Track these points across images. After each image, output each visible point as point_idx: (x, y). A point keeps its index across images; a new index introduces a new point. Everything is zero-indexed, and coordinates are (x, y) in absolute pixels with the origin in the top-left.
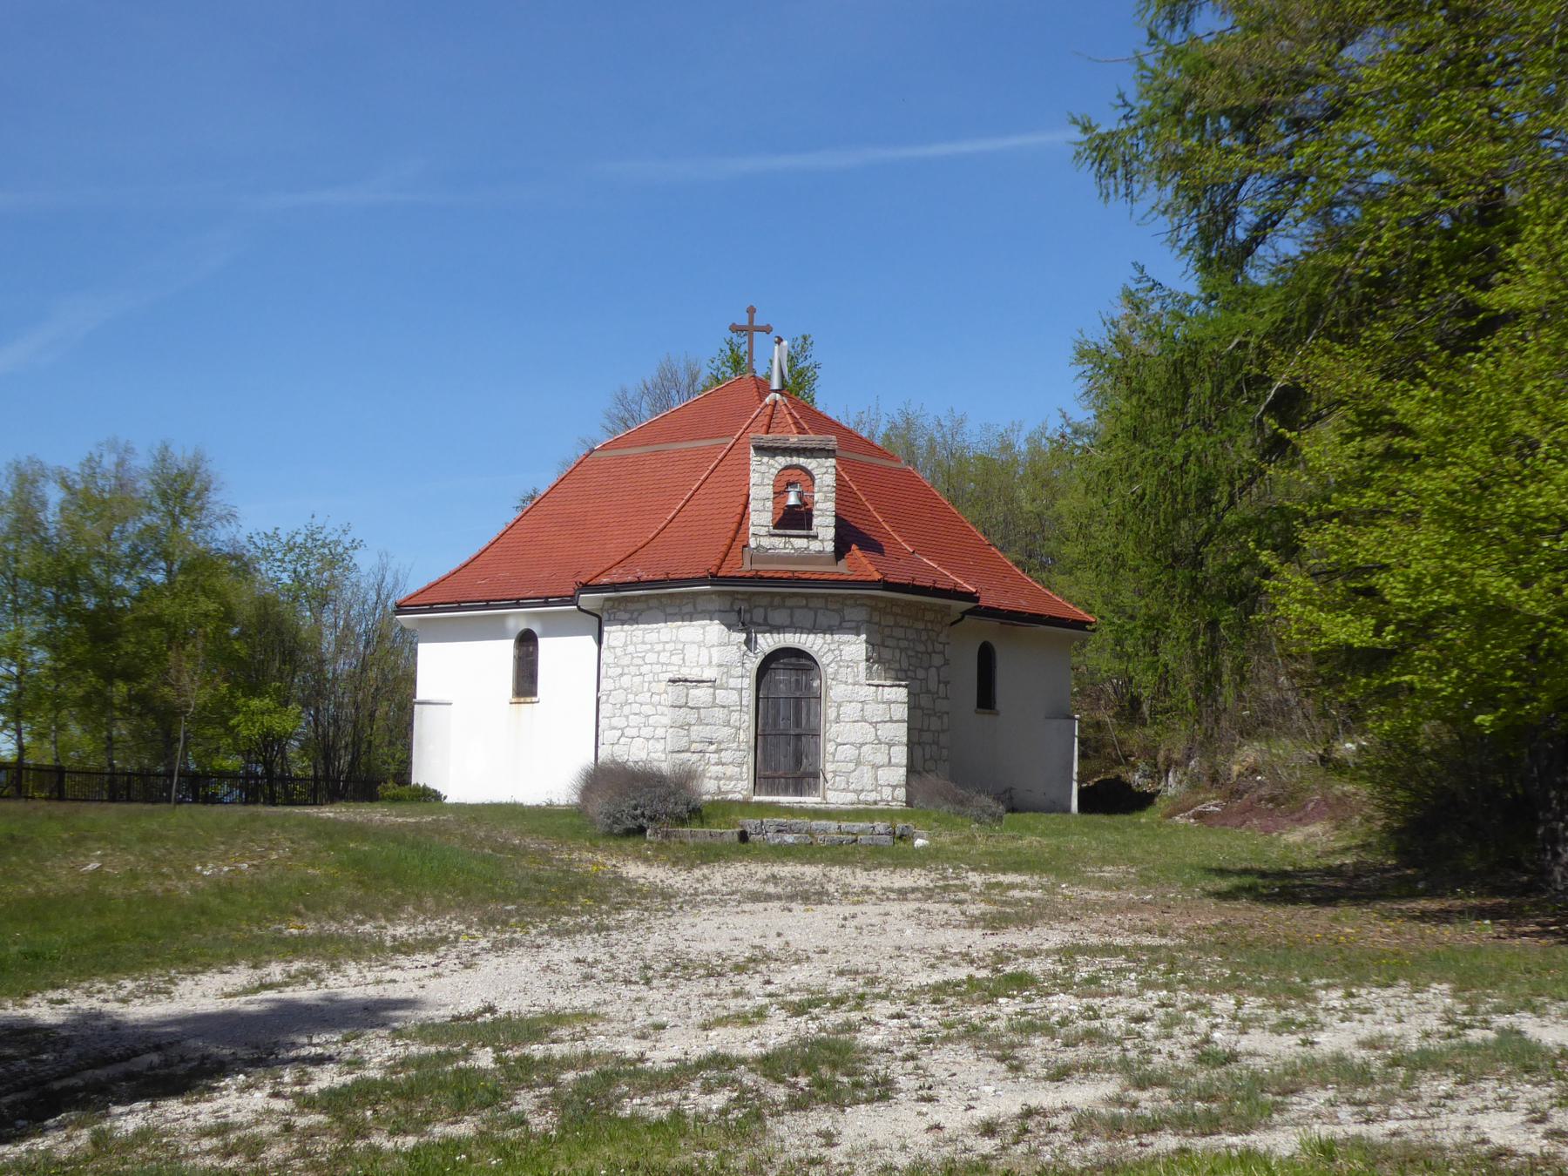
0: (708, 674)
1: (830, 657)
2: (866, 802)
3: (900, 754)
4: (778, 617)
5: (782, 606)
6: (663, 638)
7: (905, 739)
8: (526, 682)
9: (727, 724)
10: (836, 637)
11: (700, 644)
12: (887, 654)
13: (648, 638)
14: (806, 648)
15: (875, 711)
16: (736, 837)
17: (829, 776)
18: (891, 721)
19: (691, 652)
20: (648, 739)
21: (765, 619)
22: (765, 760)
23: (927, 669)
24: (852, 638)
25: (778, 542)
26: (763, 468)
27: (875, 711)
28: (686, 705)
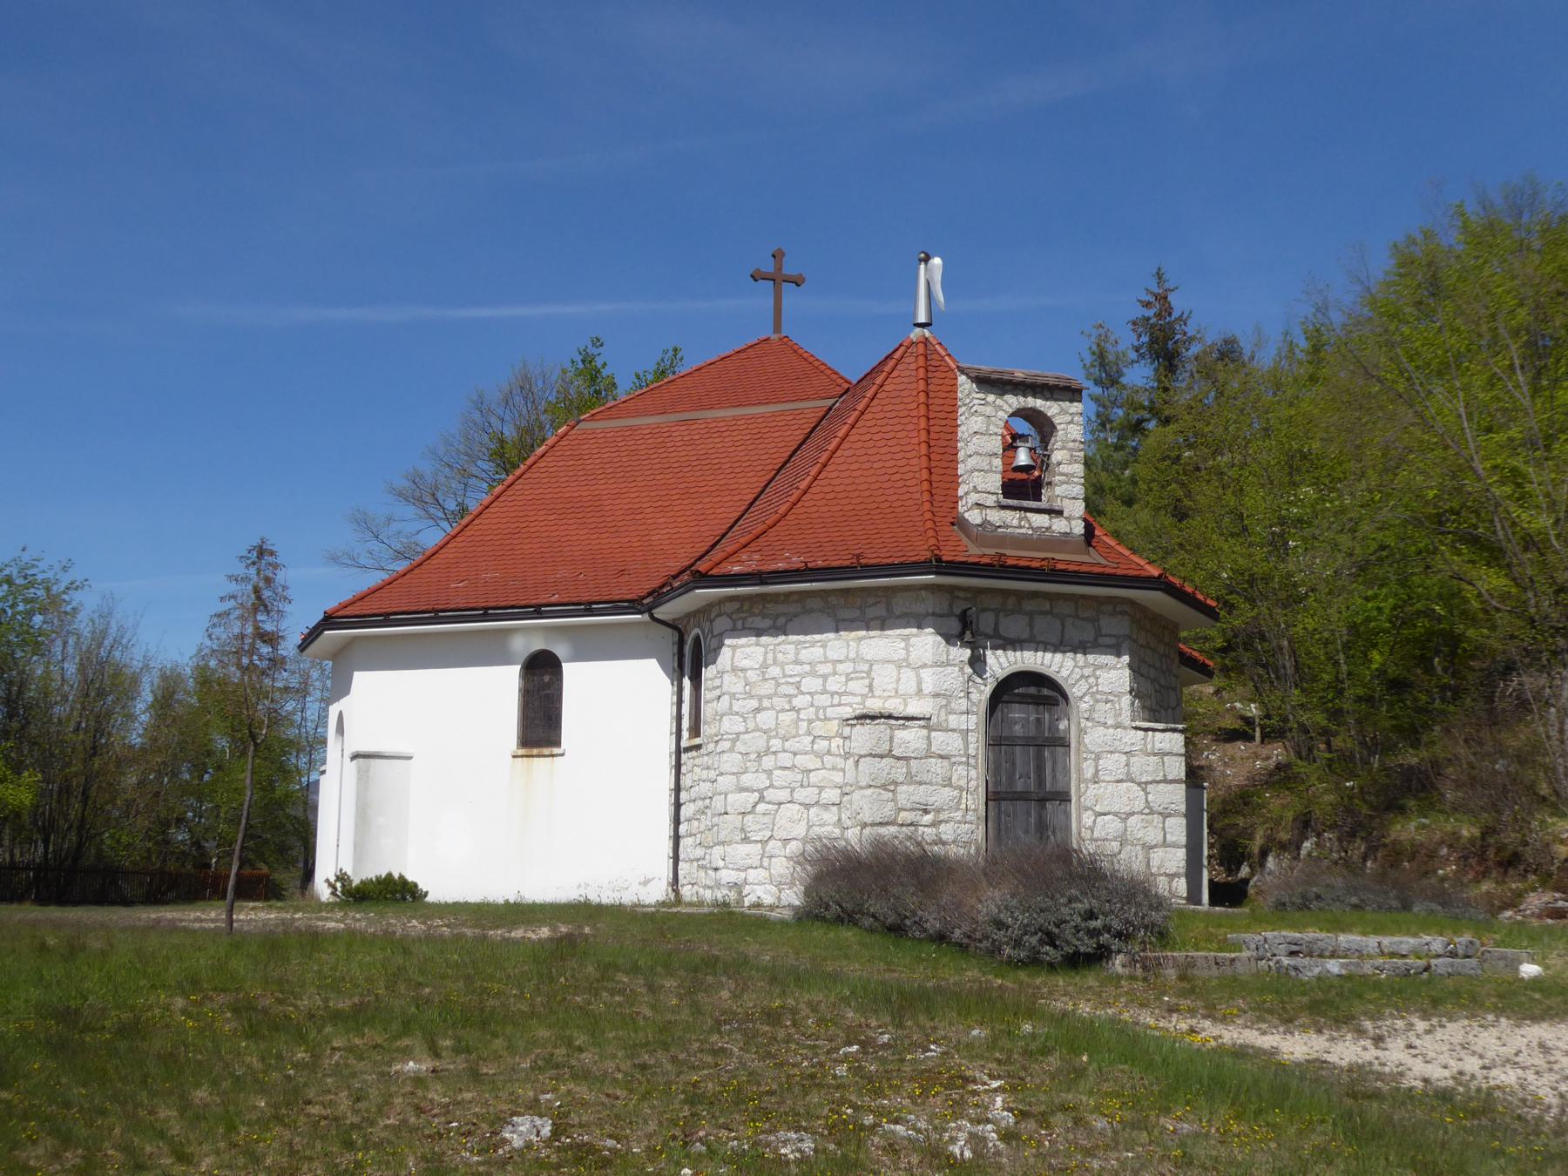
0: (913, 709)
4: (1014, 626)
6: (832, 655)
8: (540, 724)
9: (948, 783)
10: (1091, 658)
13: (805, 654)
14: (1050, 673)
15: (1145, 767)
18: (1165, 781)
19: (885, 677)
21: (996, 628)
25: (1012, 518)
26: (988, 410)
27: (1145, 767)
28: (889, 754)
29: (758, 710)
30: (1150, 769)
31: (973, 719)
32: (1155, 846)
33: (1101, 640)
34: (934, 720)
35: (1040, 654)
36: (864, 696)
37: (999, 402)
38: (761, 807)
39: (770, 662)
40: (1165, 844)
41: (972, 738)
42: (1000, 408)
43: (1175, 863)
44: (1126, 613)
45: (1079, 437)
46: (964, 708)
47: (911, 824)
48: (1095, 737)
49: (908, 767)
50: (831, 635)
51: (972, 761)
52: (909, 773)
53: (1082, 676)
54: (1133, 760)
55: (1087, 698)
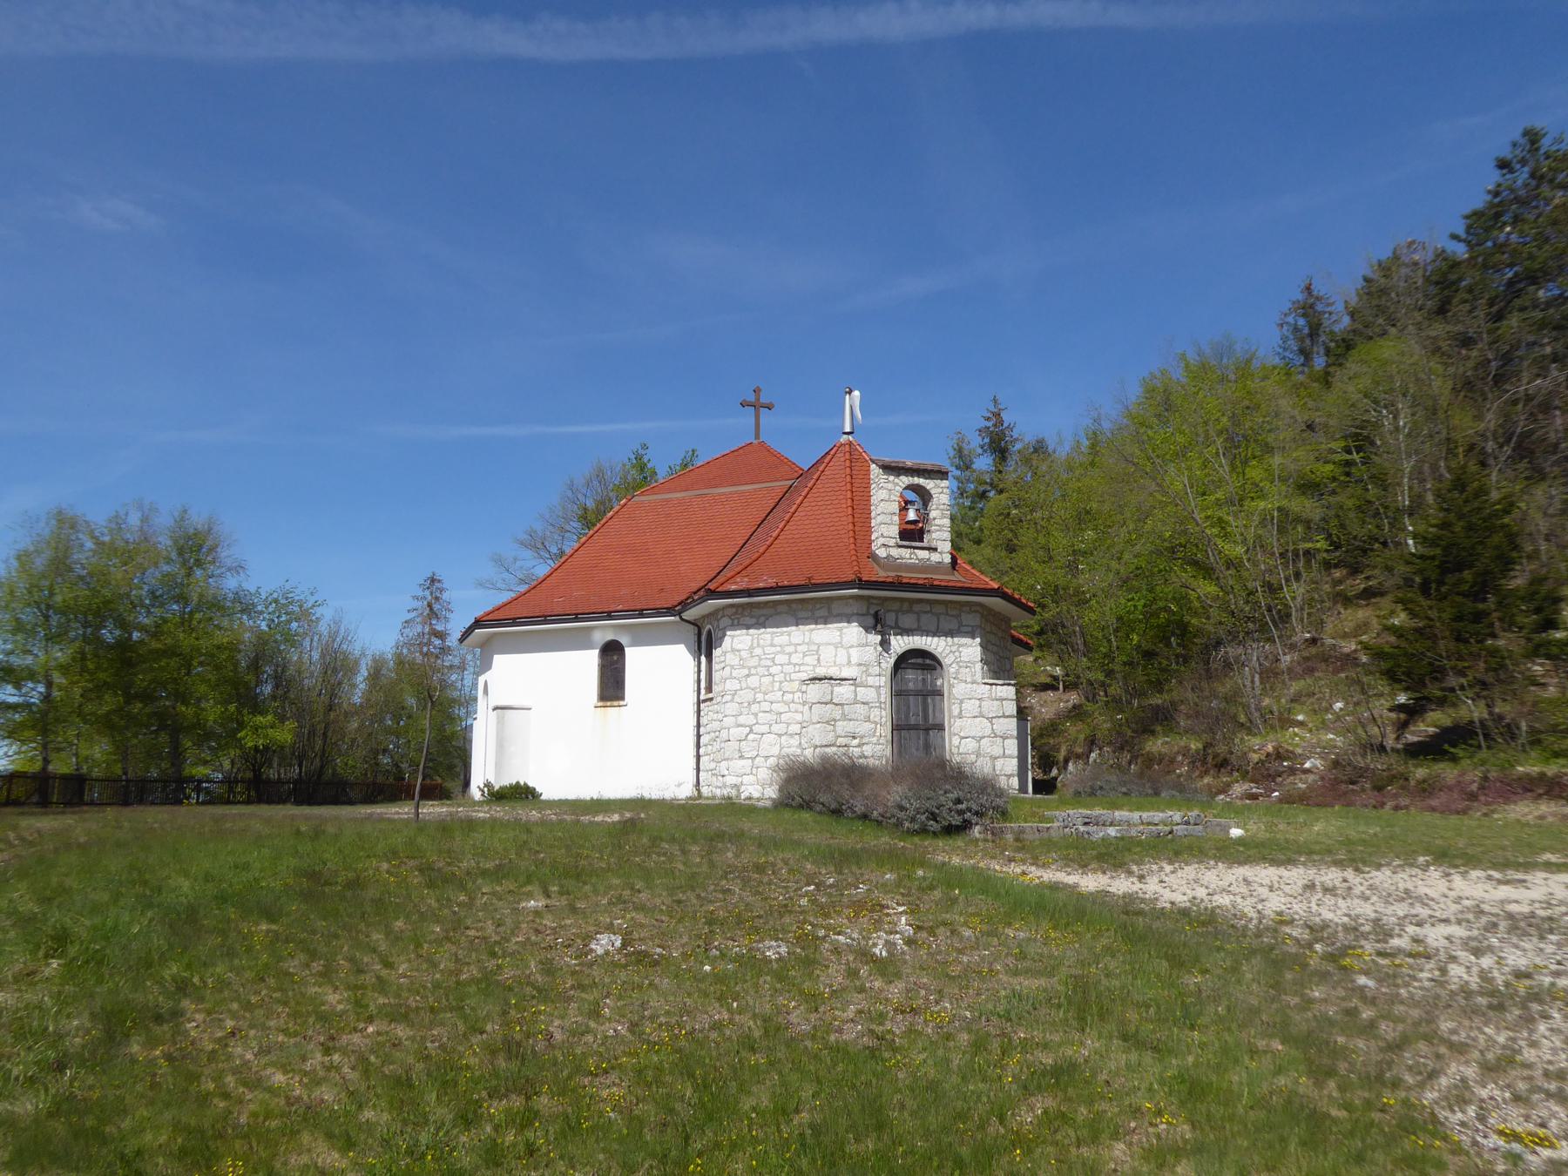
0: (844, 674)
4: (907, 620)
5: (910, 611)
6: (795, 640)
8: (612, 686)
9: (868, 719)
13: (777, 640)
14: (931, 649)
15: (991, 708)
19: (827, 653)
20: (780, 735)
25: (905, 553)
26: (890, 486)
27: (991, 708)
28: (831, 702)
38: (751, 737)
40: (1004, 756)
41: (883, 691)
48: (959, 690)
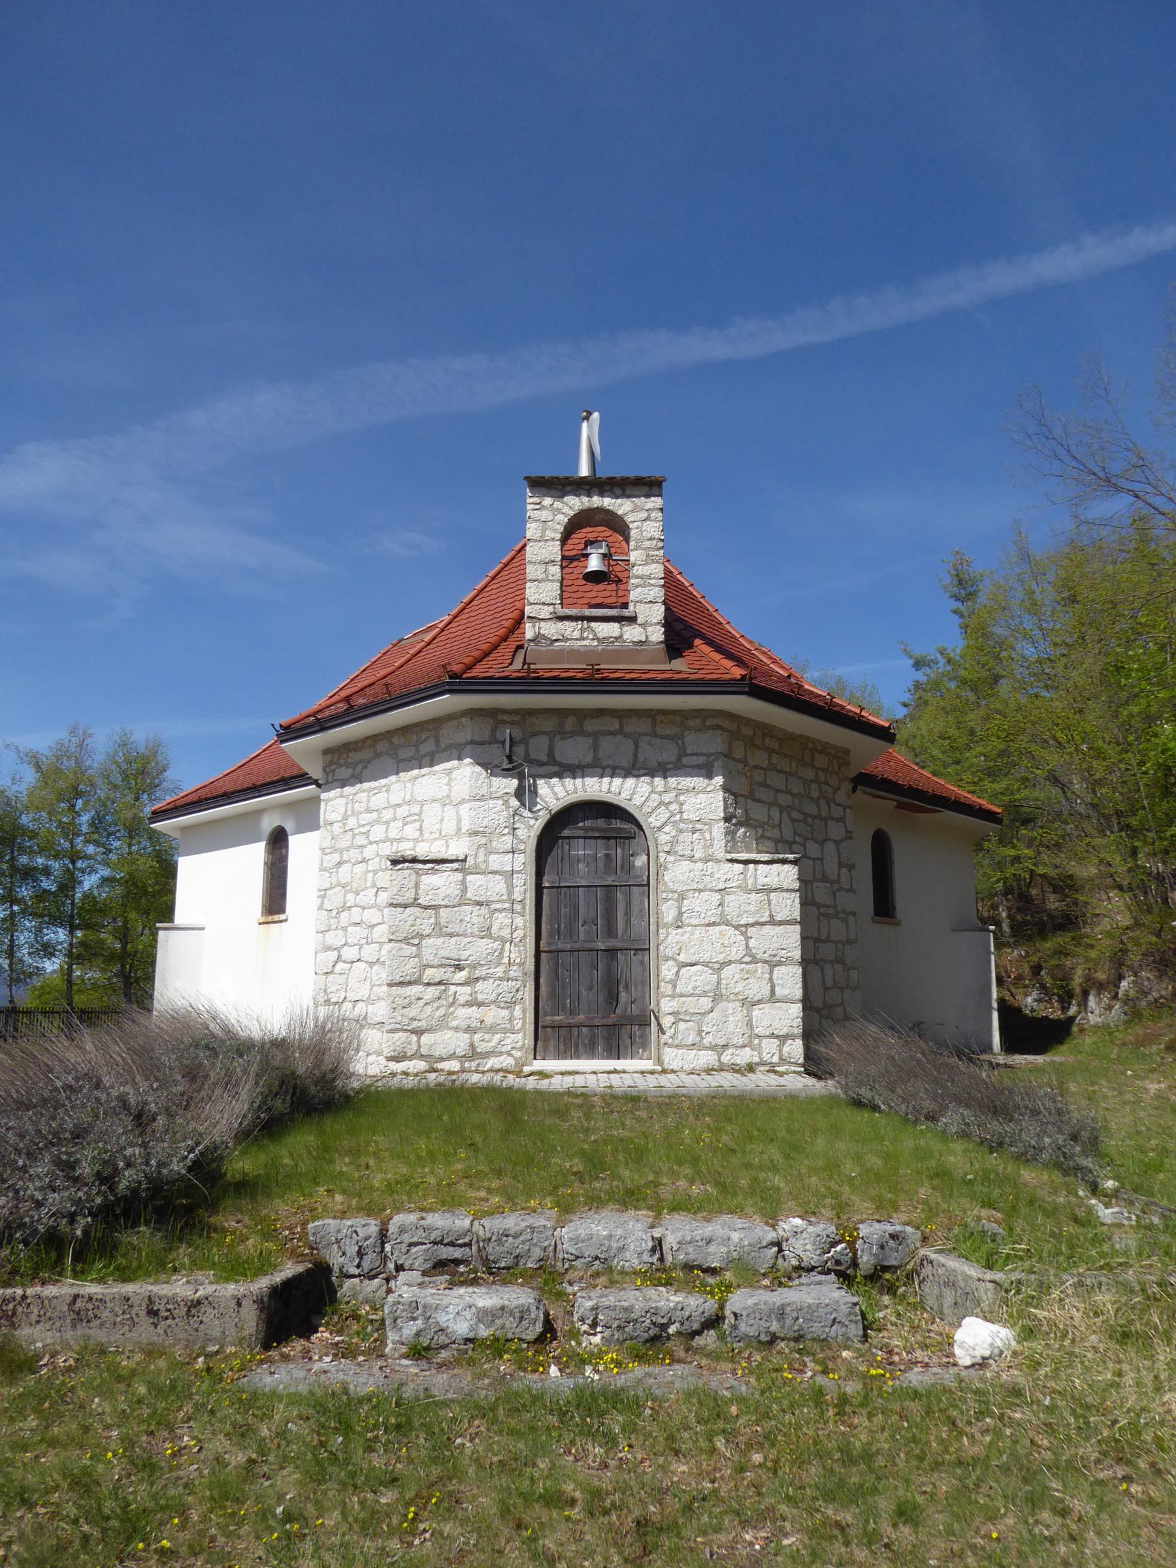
0: (456, 849)
1: (663, 814)
2: (735, 1069)
3: (790, 980)
4: (573, 750)
7: (797, 954)
9: (486, 933)
10: (672, 781)
11: (445, 802)
12: (759, 812)
14: (620, 800)
16: (251, 1319)
17: (666, 1021)
18: (772, 922)
19: (432, 814)
20: (371, 964)
21: (551, 754)
22: (555, 996)
23: (822, 843)
24: (699, 782)
26: (545, 515)
28: (415, 903)
29: (340, 864)
30: (752, 908)
31: (521, 858)
32: (760, 1002)
33: (685, 760)
34: (470, 861)
35: (606, 780)
36: (416, 840)
37: (558, 504)
38: (340, 966)
39: (349, 813)
40: (773, 998)
41: (518, 880)
42: (559, 511)
43: (788, 1022)
44: (719, 727)
45: (657, 535)
46: (508, 847)
47: (440, 983)
48: (675, 874)
49: (437, 916)
50: (393, 778)
51: (517, 907)
52: (437, 923)
53: (661, 803)
54: (728, 898)
55: (667, 829)
